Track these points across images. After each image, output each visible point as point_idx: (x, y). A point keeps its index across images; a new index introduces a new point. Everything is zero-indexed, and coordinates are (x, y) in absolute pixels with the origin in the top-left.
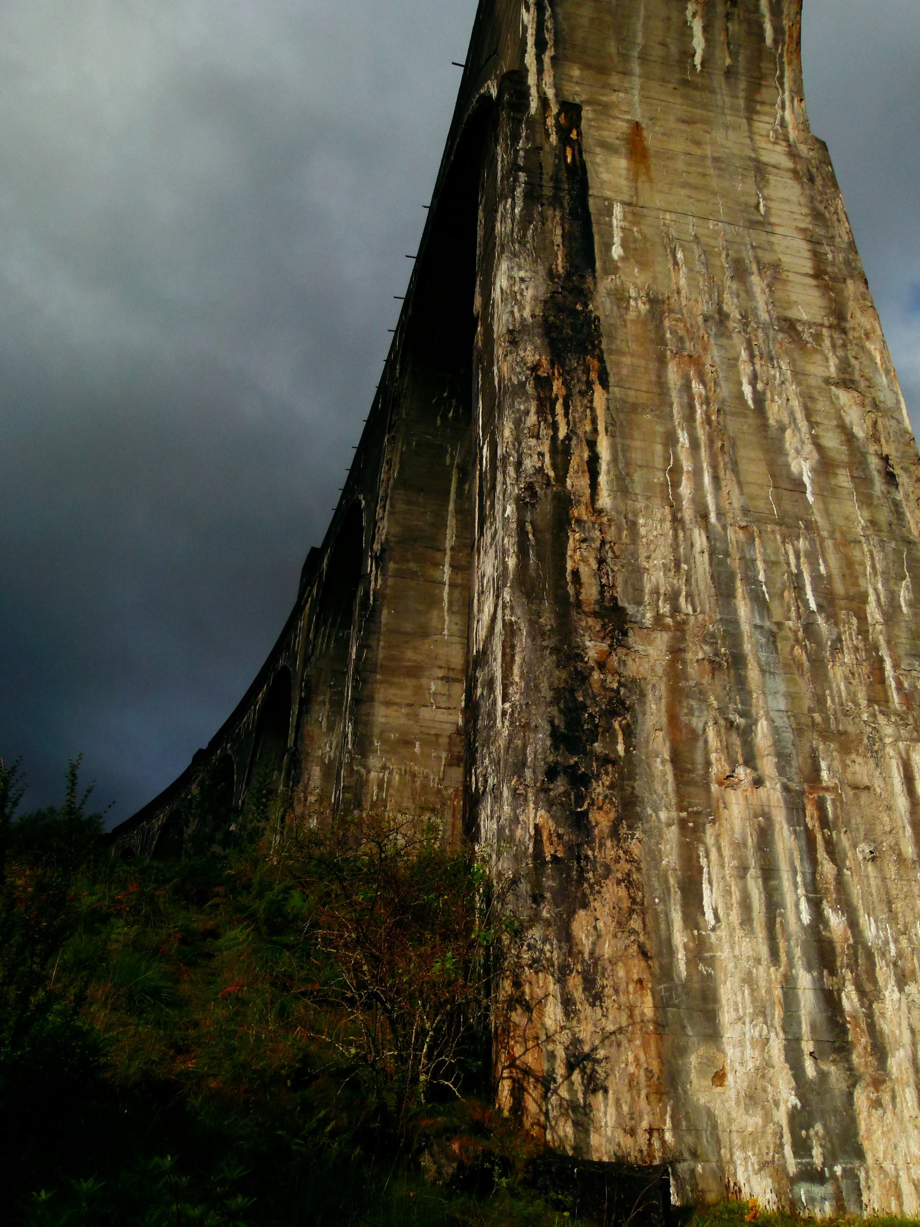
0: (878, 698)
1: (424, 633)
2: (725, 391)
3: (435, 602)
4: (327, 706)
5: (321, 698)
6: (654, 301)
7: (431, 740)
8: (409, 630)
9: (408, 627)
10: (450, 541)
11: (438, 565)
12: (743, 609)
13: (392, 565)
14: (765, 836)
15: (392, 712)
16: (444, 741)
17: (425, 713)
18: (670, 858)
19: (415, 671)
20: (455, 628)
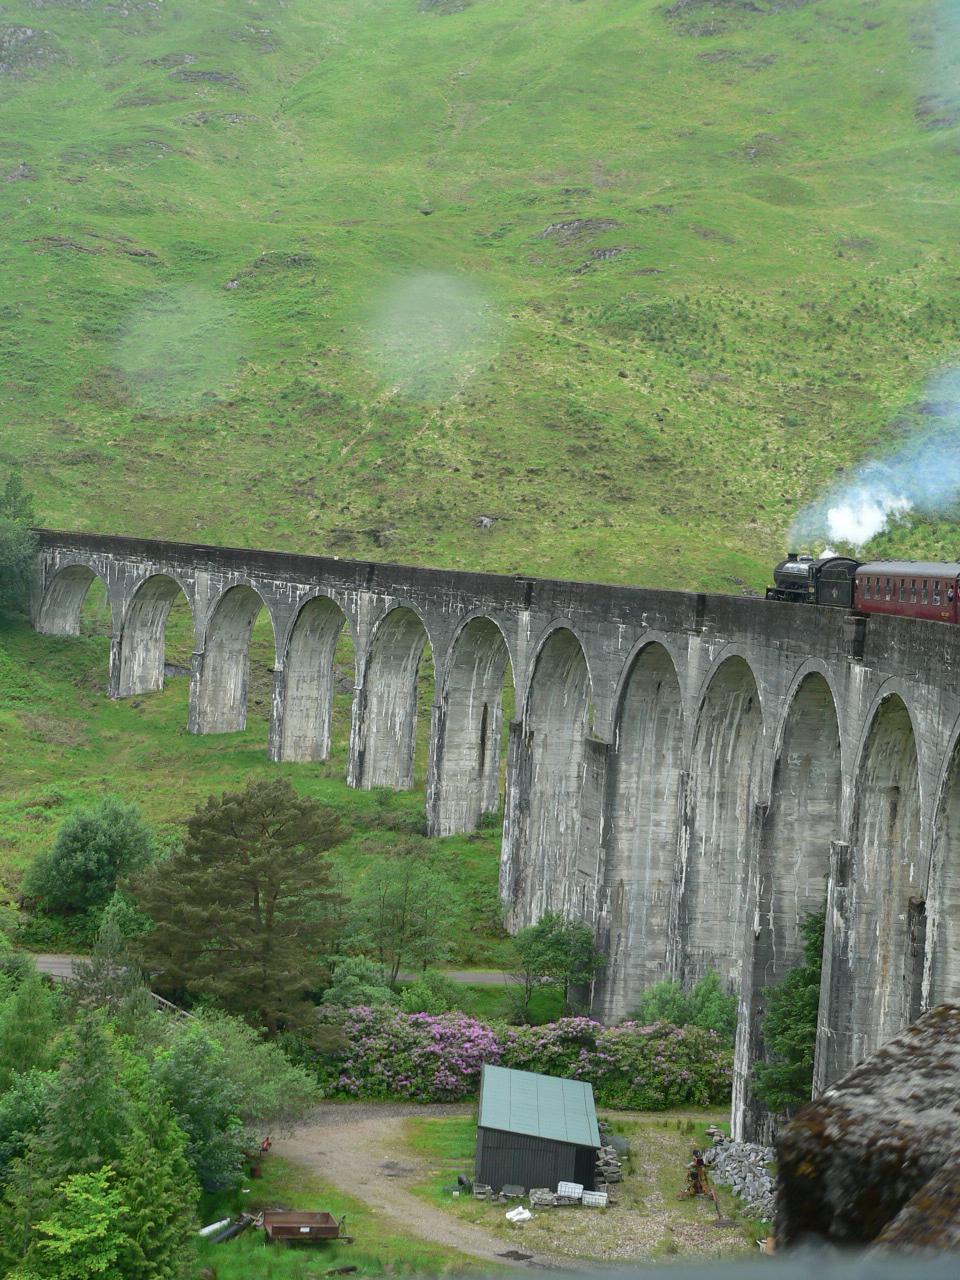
0: (564, 875)
1: (462, 729)
2: (551, 814)
6: (541, 793)
7: (463, 773)
11: (467, 698)
12: (546, 861)
13: (450, 701)
14: (542, 897)
15: (450, 763)
16: (468, 773)
17: (462, 763)
18: (529, 900)
19: (458, 746)
20: (474, 726)
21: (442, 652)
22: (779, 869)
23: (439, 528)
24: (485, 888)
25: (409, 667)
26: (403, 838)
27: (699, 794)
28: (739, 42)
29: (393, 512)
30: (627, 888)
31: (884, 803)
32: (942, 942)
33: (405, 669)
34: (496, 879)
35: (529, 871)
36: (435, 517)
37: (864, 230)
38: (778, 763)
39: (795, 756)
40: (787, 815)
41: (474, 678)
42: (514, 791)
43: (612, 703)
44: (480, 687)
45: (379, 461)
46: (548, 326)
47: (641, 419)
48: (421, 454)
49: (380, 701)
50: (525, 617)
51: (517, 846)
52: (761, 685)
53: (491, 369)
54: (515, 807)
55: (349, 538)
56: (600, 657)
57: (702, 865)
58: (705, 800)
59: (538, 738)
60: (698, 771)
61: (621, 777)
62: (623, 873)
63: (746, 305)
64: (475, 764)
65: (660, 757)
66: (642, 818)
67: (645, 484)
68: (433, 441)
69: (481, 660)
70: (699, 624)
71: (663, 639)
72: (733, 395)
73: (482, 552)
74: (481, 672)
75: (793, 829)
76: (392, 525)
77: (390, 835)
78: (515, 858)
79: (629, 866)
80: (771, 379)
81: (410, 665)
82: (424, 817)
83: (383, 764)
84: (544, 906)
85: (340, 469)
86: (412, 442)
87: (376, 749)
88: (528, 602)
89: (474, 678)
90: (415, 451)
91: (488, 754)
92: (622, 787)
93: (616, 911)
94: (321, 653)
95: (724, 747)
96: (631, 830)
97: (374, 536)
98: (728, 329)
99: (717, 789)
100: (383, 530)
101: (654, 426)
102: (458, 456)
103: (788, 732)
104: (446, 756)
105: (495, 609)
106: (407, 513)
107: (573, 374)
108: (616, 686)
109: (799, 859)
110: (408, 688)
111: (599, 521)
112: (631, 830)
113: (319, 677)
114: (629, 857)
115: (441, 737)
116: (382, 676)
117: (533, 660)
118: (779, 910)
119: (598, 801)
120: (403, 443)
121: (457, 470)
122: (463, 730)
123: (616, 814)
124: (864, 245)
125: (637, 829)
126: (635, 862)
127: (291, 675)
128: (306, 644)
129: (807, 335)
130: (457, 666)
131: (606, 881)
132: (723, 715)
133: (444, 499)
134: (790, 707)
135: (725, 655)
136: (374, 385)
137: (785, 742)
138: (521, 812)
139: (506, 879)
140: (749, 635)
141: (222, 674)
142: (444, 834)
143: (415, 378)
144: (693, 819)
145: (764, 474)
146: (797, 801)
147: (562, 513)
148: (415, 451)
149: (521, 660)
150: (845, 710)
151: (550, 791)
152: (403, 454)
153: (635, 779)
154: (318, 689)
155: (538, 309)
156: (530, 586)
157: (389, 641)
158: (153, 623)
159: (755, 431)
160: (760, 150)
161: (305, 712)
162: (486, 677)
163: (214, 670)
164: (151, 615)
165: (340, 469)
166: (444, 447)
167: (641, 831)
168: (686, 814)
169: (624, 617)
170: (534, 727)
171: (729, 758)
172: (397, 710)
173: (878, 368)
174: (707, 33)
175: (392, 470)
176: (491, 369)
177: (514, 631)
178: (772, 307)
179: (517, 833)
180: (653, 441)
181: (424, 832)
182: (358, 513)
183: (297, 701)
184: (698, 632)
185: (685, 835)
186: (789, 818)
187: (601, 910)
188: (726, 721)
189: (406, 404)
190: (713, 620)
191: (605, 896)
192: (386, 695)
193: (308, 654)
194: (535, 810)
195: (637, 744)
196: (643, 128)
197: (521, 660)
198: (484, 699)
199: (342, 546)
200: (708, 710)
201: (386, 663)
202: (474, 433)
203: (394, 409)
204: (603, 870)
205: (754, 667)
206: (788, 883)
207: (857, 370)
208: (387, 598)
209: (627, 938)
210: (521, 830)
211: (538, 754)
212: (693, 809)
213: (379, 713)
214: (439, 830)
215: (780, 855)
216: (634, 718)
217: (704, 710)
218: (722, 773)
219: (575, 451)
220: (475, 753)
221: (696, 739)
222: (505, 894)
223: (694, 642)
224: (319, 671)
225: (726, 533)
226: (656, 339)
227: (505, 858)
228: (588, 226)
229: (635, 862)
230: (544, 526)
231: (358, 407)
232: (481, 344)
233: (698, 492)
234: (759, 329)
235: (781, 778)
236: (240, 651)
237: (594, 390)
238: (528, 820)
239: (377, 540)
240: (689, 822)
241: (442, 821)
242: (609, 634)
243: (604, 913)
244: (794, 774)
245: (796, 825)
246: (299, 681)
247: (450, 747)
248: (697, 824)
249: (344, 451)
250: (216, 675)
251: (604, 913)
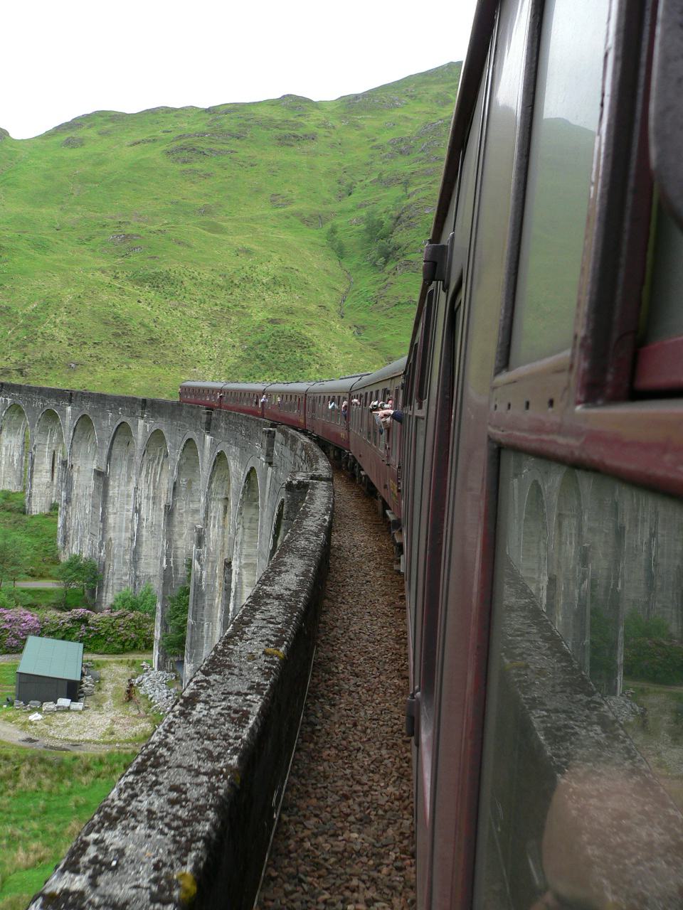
1: (42, 463)
3: (44, 456)
10: (48, 443)
19: (41, 471)
21: (33, 426)
22: (176, 537)
23: (51, 368)
24: (51, 540)
26: (14, 515)
27: (143, 497)
28: (197, 166)
29: (30, 360)
30: (113, 542)
31: (221, 506)
32: (240, 582)
33: (19, 434)
34: (55, 535)
35: (71, 532)
36: (49, 363)
37: (247, 245)
38: (175, 483)
39: (184, 480)
40: (179, 509)
41: (48, 438)
42: (63, 494)
43: (106, 451)
44: (51, 442)
45: (25, 337)
46: (107, 280)
47: (146, 321)
48: (45, 335)
49: (6, 449)
50: (69, 409)
51: (65, 520)
52: (169, 444)
53: (79, 297)
54: (64, 501)
55: (8, 372)
56: (101, 429)
57: (144, 532)
58: (146, 500)
59: (75, 468)
60: (142, 486)
61: (110, 488)
62: (111, 534)
63: (196, 273)
64: (49, 480)
65: (129, 478)
66: (120, 507)
67: (147, 351)
68: (51, 329)
69: (51, 430)
70: (143, 413)
71: (128, 420)
72: (188, 312)
73: (70, 379)
75: (182, 517)
76: (29, 367)
77: (8, 514)
78: (64, 526)
79: (114, 531)
80: (206, 307)
81: (21, 431)
82: (24, 506)
83: (8, 479)
84: (79, 549)
85: (7, 340)
86: (41, 329)
87: (5, 471)
88: (70, 401)
89: (48, 438)
90: (42, 333)
91: (55, 474)
92: (111, 493)
93: (108, 553)
95: (155, 474)
96: (115, 514)
97: (21, 371)
98: (187, 283)
99: (152, 495)
100: (25, 369)
101: (152, 325)
102: (61, 335)
103: (180, 468)
104: (35, 476)
105: (56, 405)
106: (36, 361)
107: (116, 300)
108: (107, 443)
109: (186, 531)
110: (20, 443)
111: (125, 366)
112: (115, 514)
114: (114, 527)
115: (32, 467)
117: (73, 430)
118: (176, 557)
119: (99, 500)
120: (36, 329)
121: (61, 342)
123: (108, 506)
124: (248, 252)
125: (118, 513)
126: (117, 529)
129: (222, 288)
130: (39, 433)
131: (103, 538)
132: (154, 459)
133: (54, 355)
134: (180, 456)
135: (154, 429)
136: (25, 303)
137: (179, 473)
138: (67, 503)
139: (60, 536)
140: (164, 419)
142: (33, 514)
143: (44, 300)
144: (140, 510)
145: (201, 347)
146: (184, 502)
147: (108, 362)
148: (42, 333)
149: (67, 430)
150: (202, 458)
152: (36, 334)
153: (117, 489)
155: (103, 272)
156: (71, 394)
157: (10, 420)
159: (198, 328)
160: (206, 211)
165: (7, 340)
166: (55, 332)
167: (120, 514)
168: (136, 507)
169: (111, 409)
170: (73, 462)
171: (158, 480)
173: (252, 303)
174: (184, 162)
175: (31, 342)
176: (79, 297)
177: (64, 416)
178: (207, 276)
179: (65, 513)
180: (151, 331)
181: (24, 513)
182: (14, 361)
184: (142, 417)
185: (136, 518)
186: (181, 511)
187: (100, 552)
188: (156, 462)
189: (39, 312)
190: (149, 412)
191: (102, 546)
194: (73, 502)
195: (118, 472)
196: (156, 199)
197: (67, 430)
198: (53, 449)
199: (5, 376)
200: (147, 456)
201: (9, 431)
202: (70, 325)
203: (34, 313)
204: (101, 533)
205: (166, 435)
206: (180, 543)
207: (244, 304)
208: (8, 399)
209: (113, 566)
210: (67, 512)
211: (75, 476)
212: (140, 505)
213: (6, 455)
214: (31, 512)
215: (176, 529)
216: (116, 459)
217: (145, 456)
218: (154, 487)
219: (116, 335)
220: (49, 475)
221: (141, 470)
222: (59, 544)
223: (141, 422)
225: (182, 373)
226: (155, 286)
227: (59, 526)
228: (127, 237)
229: (117, 529)
230: (100, 368)
231: (17, 313)
232: (76, 286)
233: (171, 354)
234: (201, 284)
235: (177, 491)
237: (126, 307)
238: (70, 508)
239: (22, 373)
240: (137, 511)
241: (33, 507)
242: (105, 417)
243: (102, 554)
244: (183, 489)
245: (184, 515)
247: (36, 472)
248: (142, 512)
249: (9, 332)
251: (102, 554)
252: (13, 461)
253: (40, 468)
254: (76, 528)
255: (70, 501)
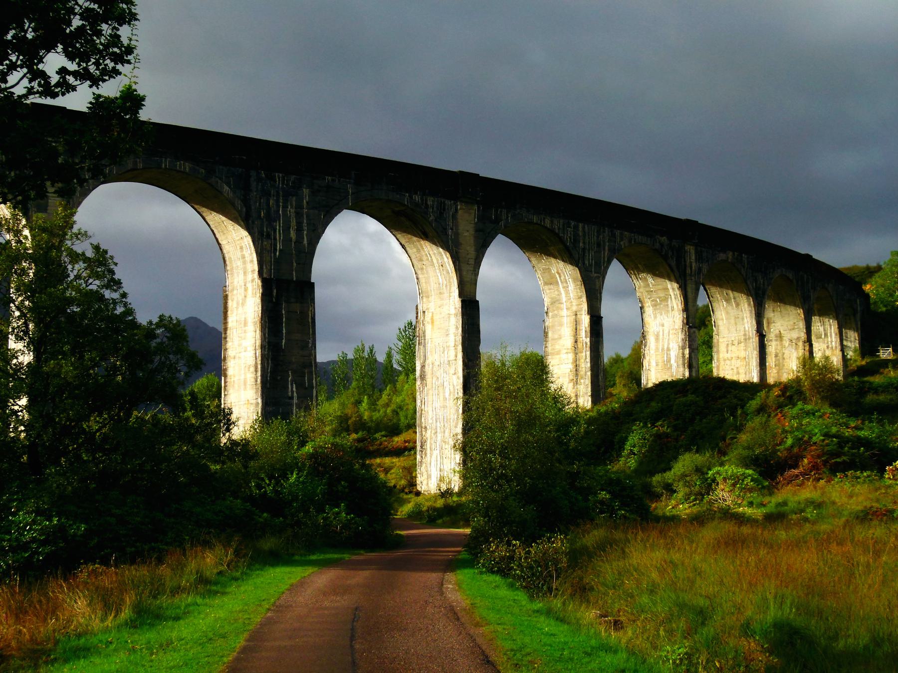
4: (651, 307)
5: (647, 305)
8: (556, 338)
9: (556, 336)
16: (567, 375)
19: (558, 353)
25: (675, 307)
33: (673, 310)
49: (657, 339)
59: (428, 316)
74: (565, 285)
94: (743, 319)
113: (745, 339)
116: (655, 317)
122: (560, 338)
127: (721, 340)
128: (727, 313)
141: (784, 359)
151: (437, 363)
154: (745, 350)
158: (826, 335)
161: (735, 370)
162: (570, 288)
163: (776, 356)
164: (821, 329)
172: (671, 346)
183: (728, 362)
192: (661, 334)
193: (733, 321)
198: (574, 308)
201: (655, 306)
213: (657, 349)
220: (571, 356)
224: (745, 335)
236: (798, 338)
246: (728, 345)
247: (553, 354)
250: (779, 360)
252: (669, 360)
253: (557, 347)
254: (434, 427)
255: (425, 376)
